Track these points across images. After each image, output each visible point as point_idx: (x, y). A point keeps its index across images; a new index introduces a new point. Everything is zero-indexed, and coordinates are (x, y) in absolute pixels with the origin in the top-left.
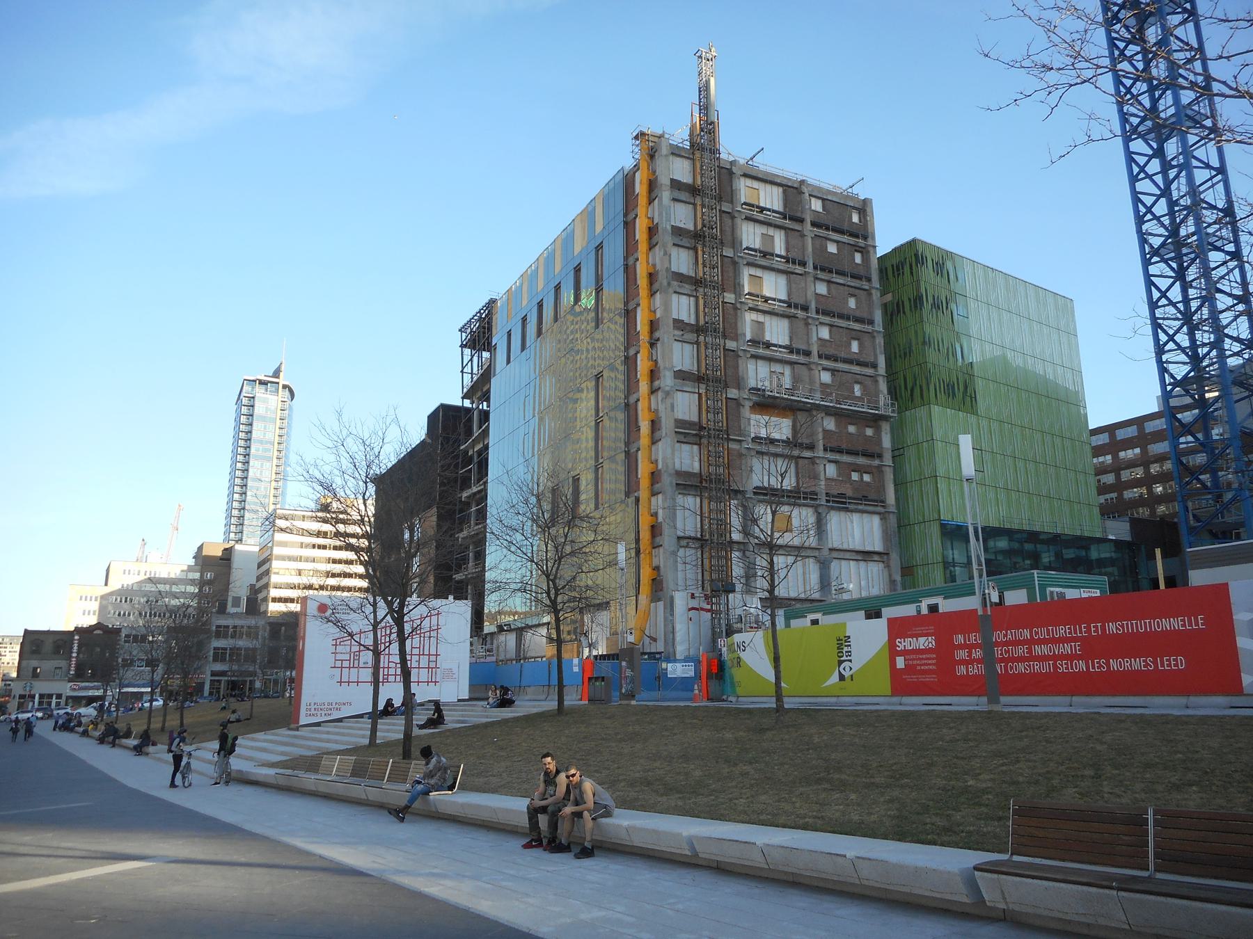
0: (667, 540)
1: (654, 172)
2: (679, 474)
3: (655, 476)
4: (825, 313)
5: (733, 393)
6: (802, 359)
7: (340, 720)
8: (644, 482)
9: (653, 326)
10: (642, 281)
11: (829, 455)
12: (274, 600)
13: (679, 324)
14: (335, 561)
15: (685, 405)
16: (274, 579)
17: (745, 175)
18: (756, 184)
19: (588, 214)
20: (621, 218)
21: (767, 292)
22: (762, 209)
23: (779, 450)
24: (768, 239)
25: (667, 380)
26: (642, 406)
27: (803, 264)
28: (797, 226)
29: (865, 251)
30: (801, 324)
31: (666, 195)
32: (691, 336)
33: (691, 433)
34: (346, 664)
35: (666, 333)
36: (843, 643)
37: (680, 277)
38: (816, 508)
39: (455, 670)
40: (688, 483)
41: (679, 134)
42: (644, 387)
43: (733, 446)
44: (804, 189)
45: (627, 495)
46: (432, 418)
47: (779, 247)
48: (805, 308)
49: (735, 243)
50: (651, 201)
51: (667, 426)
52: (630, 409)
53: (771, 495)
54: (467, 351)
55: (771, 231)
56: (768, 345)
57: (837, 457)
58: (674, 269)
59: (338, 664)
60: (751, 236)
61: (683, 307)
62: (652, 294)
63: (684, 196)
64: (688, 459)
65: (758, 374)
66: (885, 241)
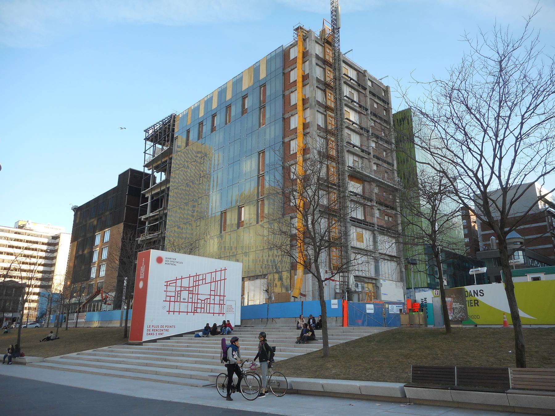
7: (168, 338)
20: (281, 70)
29: (388, 110)
30: (365, 139)
34: (173, 299)
39: (234, 307)
46: (122, 177)
50: (304, 62)
59: (168, 299)
66: (397, 106)
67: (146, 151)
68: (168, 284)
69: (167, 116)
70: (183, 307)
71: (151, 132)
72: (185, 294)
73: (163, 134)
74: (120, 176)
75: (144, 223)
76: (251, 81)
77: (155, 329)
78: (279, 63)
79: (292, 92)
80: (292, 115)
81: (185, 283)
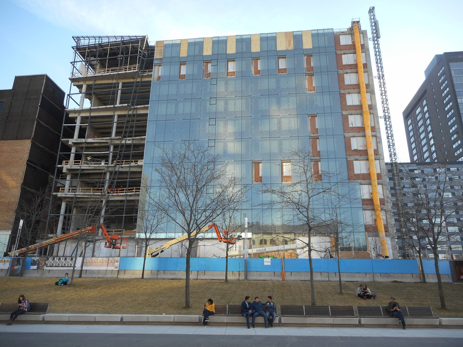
67: (74, 62)
69: (131, 34)
71: (84, 42)
76: (289, 45)
79: (347, 73)
80: (349, 93)
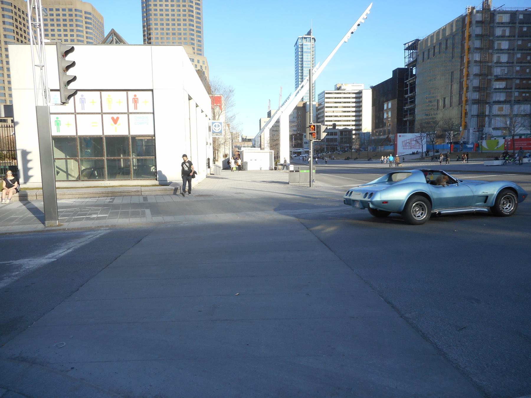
0: (469, 116)
1: (471, 19)
2: (473, 100)
3: (467, 101)
4: (519, 50)
5: (489, 77)
6: (511, 65)
8: (464, 102)
9: (469, 62)
10: (466, 51)
11: (516, 90)
12: (326, 121)
13: (476, 62)
14: (344, 107)
15: (476, 82)
16: (326, 114)
17: (499, 13)
18: (501, 15)
19: (451, 24)
21: (503, 47)
22: (502, 23)
23: (501, 91)
24: (504, 31)
25: (471, 77)
26: (464, 83)
27: (514, 36)
28: (513, 25)
31: (474, 27)
32: (479, 64)
33: (477, 89)
35: (472, 64)
36: (498, 142)
37: (477, 49)
38: (511, 105)
40: (476, 102)
41: (479, 7)
42: (465, 79)
43: (488, 91)
44: (517, 13)
45: (459, 104)
46: (394, 72)
47: (507, 34)
48: (513, 50)
49: (493, 35)
51: (471, 88)
52: (461, 83)
53: (499, 102)
54: (407, 51)
55: (505, 28)
56: (501, 63)
57: (519, 90)
58: (475, 46)
60: (498, 32)
61: (477, 57)
62: (469, 53)
63: (479, 25)
64: (476, 96)
65: (497, 71)
68: (403, 142)
70: (407, 147)
72: (408, 144)
73: (413, 46)
74: (393, 71)
75: (406, 99)
77: (400, 153)
78: (460, 23)
81: (408, 141)
